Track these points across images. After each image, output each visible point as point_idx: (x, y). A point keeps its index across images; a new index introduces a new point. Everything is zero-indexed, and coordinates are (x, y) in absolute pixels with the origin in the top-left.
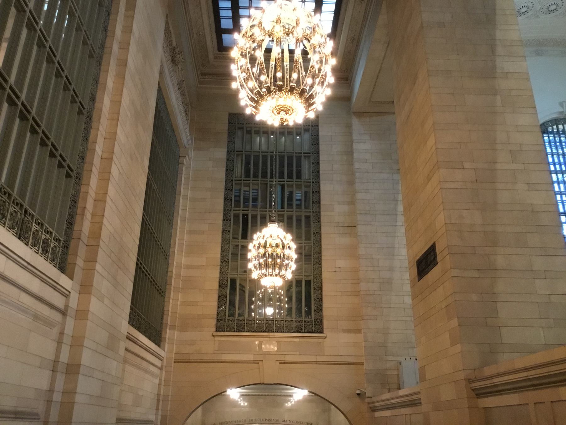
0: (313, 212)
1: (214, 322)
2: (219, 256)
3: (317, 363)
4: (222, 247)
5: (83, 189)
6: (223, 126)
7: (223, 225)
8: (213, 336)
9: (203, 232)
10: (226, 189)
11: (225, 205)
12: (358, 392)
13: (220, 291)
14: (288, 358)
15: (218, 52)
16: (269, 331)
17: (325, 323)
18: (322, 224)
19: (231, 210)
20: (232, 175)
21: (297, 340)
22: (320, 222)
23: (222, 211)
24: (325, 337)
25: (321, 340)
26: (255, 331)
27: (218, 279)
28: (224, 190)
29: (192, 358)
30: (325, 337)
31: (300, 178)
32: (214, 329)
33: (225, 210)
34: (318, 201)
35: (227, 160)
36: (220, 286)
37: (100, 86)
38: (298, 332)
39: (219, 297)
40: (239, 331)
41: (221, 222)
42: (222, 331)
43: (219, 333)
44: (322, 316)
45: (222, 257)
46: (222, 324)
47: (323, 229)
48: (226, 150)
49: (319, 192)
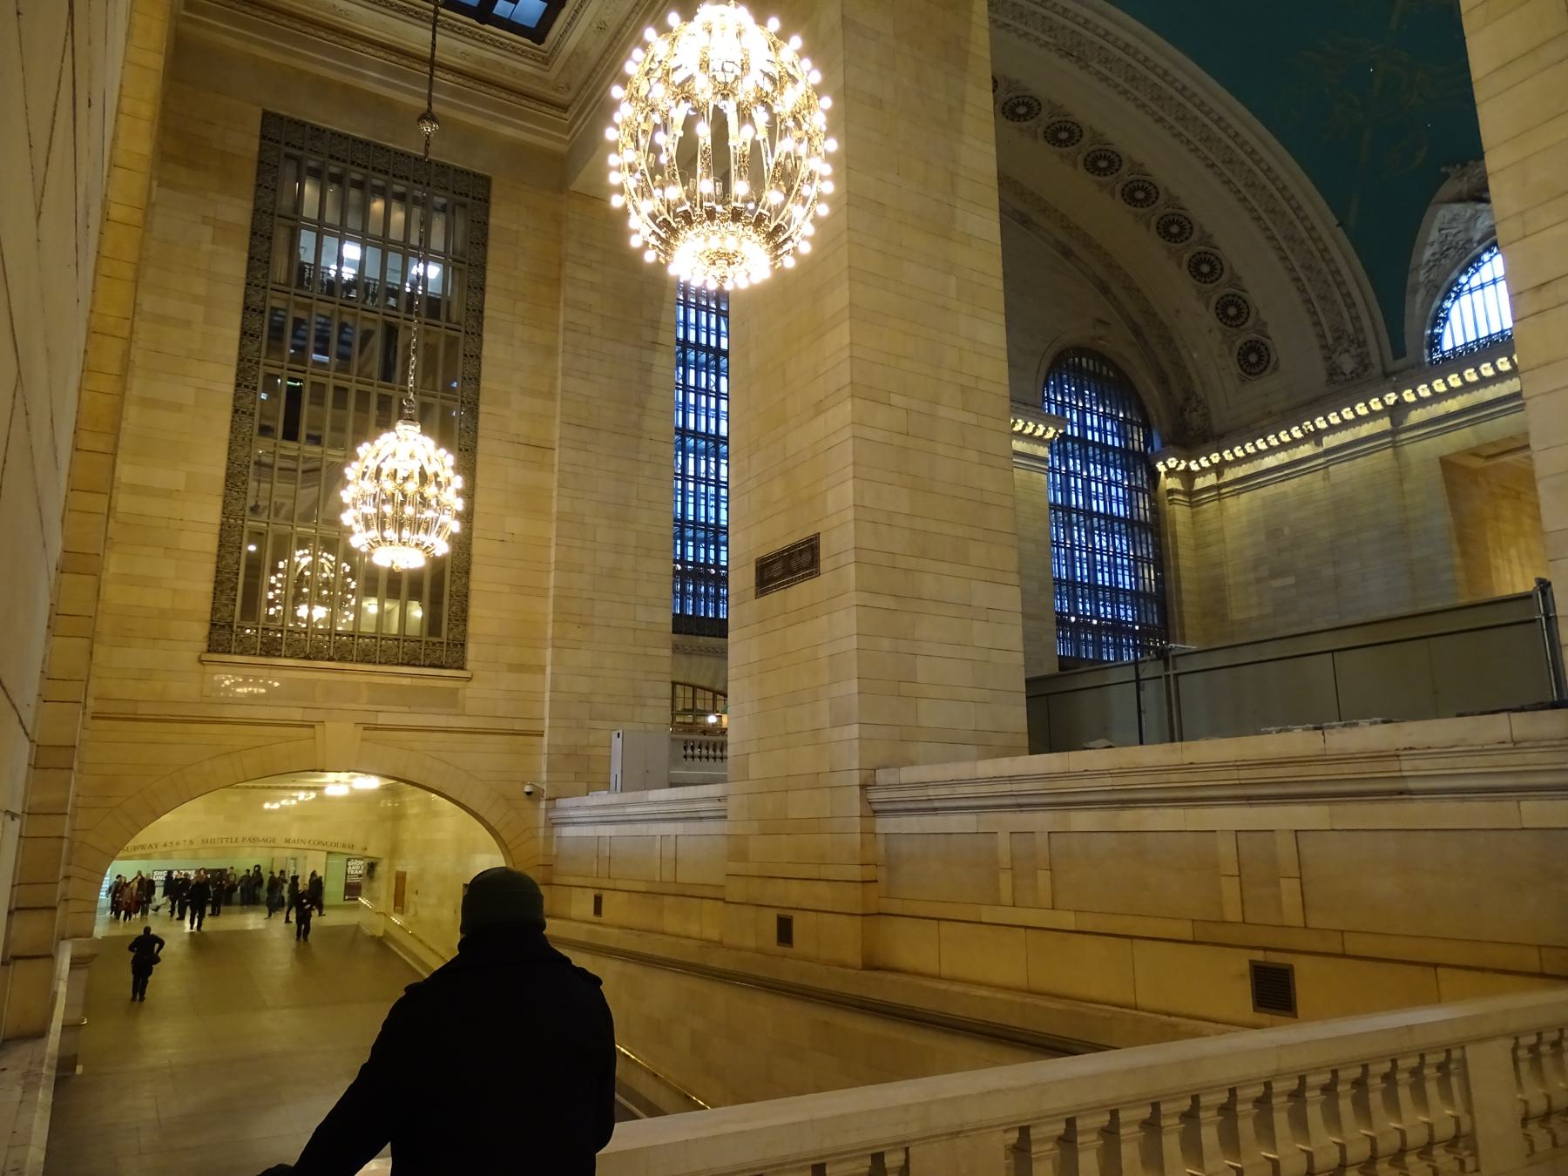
1: (200, 630)
2: (222, 473)
3: (446, 730)
4: (231, 451)
6: (246, 141)
7: (236, 398)
8: (201, 661)
9: (178, 407)
11: (242, 346)
12: (527, 789)
13: (220, 557)
14: (383, 719)
16: (342, 659)
17: (472, 650)
19: (258, 363)
20: (266, 276)
21: (406, 681)
24: (469, 679)
25: (459, 684)
26: (307, 658)
27: (217, 529)
29: (142, 710)
31: (437, 317)
32: (204, 646)
35: (254, 233)
36: (221, 546)
38: (408, 664)
39: (218, 571)
40: (268, 654)
41: (230, 389)
42: (224, 652)
43: (216, 657)
44: (464, 633)
45: (229, 476)
46: (223, 638)
48: (249, 206)
49: (478, 357)
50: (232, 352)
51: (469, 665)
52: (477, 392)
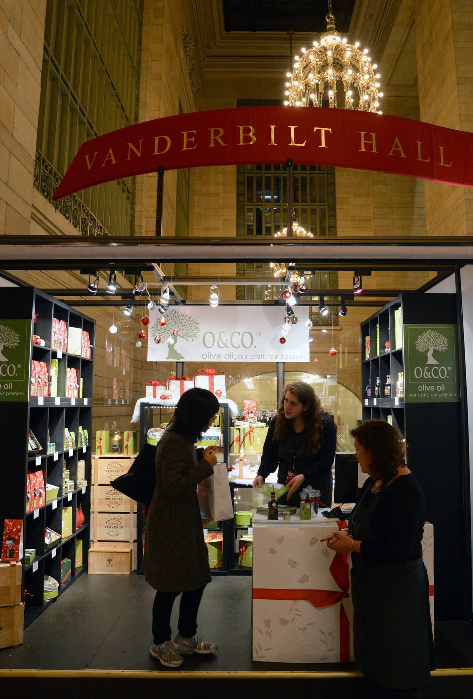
0: (328, 205)
5: (137, 208)
7: (238, 221)
10: (238, 183)
11: (238, 199)
15: (224, 32)
18: (338, 218)
19: (244, 205)
22: (335, 216)
23: (236, 206)
28: (236, 184)
30: (341, 329)
33: (238, 205)
34: (333, 195)
37: (141, 105)
47: (338, 223)
49: (334, 184)
50: (235, 203)
51: (340, 324)
52: (335, 200)
